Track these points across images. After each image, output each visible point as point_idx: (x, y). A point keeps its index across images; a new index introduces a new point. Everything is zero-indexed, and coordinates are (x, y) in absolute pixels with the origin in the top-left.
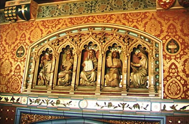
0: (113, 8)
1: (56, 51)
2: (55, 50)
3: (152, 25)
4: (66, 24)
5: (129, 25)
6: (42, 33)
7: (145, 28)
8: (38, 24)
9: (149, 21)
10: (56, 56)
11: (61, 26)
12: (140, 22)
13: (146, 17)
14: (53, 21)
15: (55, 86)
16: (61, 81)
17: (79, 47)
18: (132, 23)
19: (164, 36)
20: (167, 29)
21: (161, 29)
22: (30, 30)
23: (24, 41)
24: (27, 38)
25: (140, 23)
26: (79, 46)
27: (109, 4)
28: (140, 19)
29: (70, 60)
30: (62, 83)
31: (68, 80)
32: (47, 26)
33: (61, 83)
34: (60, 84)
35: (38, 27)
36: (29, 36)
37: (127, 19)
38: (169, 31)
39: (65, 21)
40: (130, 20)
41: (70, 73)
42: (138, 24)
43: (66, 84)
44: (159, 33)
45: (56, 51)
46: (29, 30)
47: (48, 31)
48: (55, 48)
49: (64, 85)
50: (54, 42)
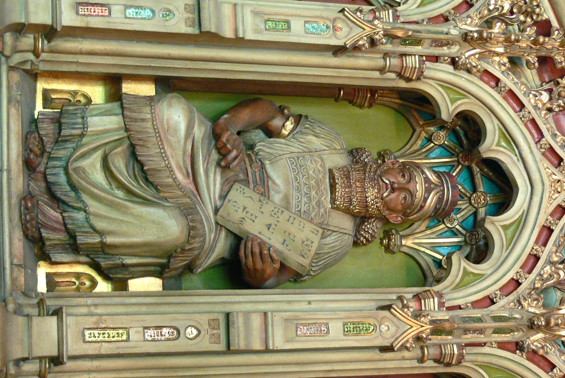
1: (448, 44)
2: (466, 37)
10: (386, 55)
15: (17, 59)
16: (89, 143)
17: (502, 346)
26: (518, 347)
29: (347, 211)
30: (62, 153)
31: (109, 240)
33: (59, 140)
34: (47, 129)
41: (197, 257)
43: (54, 214)
45: (454, 50)
48: (482, 40)
49: (38, 187)
50: (549, 15)
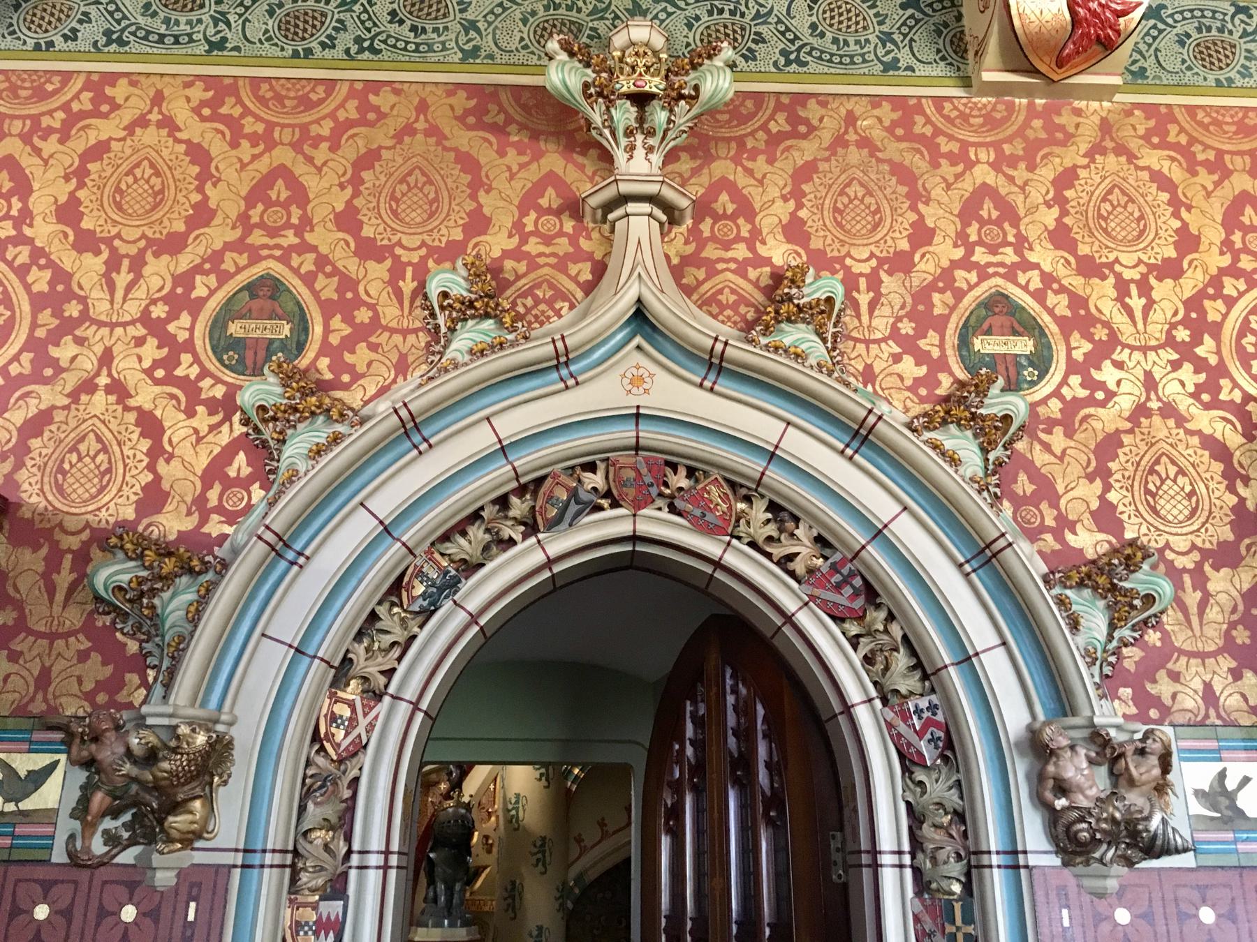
0: (807, 49)
3: (1110, 192)
4: (433, 131)
5: (945, 180)
6: (205, 177)
7: (1064, 213)
8: (158, 99)
9: (1086, 161)
11: (390, 143)
12: (1022, 165)
13: (1059, 135)
14: (314, 97)
18: (960, 168)
19: (1205, 271)
20: (1220, 228)
21: (1177, 224)
22: (79, 144)
23: (6, 230)
24: (41, 202)
25: (1021, 173)
27: (773, 19)
28: (1018, 148)
32: (250, 125)
35: (160, 125)
36: (63, 191)
37: (922, 138)
38: (1237, 237)
39: (422, 107)
40: (946, 146)
42: (1011, 179)
44: (1171, 253)
46: (62, 141)
47: (263, 165)
